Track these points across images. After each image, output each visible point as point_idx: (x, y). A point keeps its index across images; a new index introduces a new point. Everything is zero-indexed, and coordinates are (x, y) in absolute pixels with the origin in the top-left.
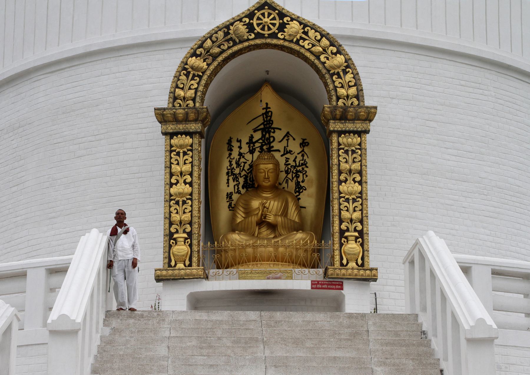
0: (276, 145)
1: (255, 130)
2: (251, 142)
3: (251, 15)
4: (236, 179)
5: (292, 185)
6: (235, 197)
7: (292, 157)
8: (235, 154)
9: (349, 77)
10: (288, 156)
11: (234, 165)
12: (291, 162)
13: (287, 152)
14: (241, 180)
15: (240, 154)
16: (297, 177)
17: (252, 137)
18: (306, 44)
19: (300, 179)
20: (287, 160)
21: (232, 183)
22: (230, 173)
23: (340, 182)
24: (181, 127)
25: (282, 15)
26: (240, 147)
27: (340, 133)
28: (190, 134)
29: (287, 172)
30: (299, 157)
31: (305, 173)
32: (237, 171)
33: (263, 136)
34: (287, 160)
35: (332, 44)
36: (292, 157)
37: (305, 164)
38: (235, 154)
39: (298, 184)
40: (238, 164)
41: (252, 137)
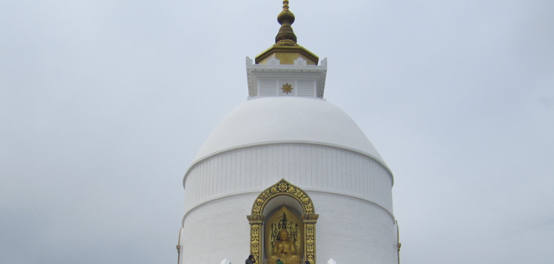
2: (279, 225)
5: (293, 239)
6: (274, 243)
7: (292, 230)
8: (274, 229)
9: (310, 205)
13: (291, 228)
14: (276, 238)
21: (273, 239)
22: (272, 235)
23: (307, 239)
25: (288, 185)
27: (307, 223)
31: (297, 235)
36: (292, 230)
38: (274, 229)
39: (294, 239)
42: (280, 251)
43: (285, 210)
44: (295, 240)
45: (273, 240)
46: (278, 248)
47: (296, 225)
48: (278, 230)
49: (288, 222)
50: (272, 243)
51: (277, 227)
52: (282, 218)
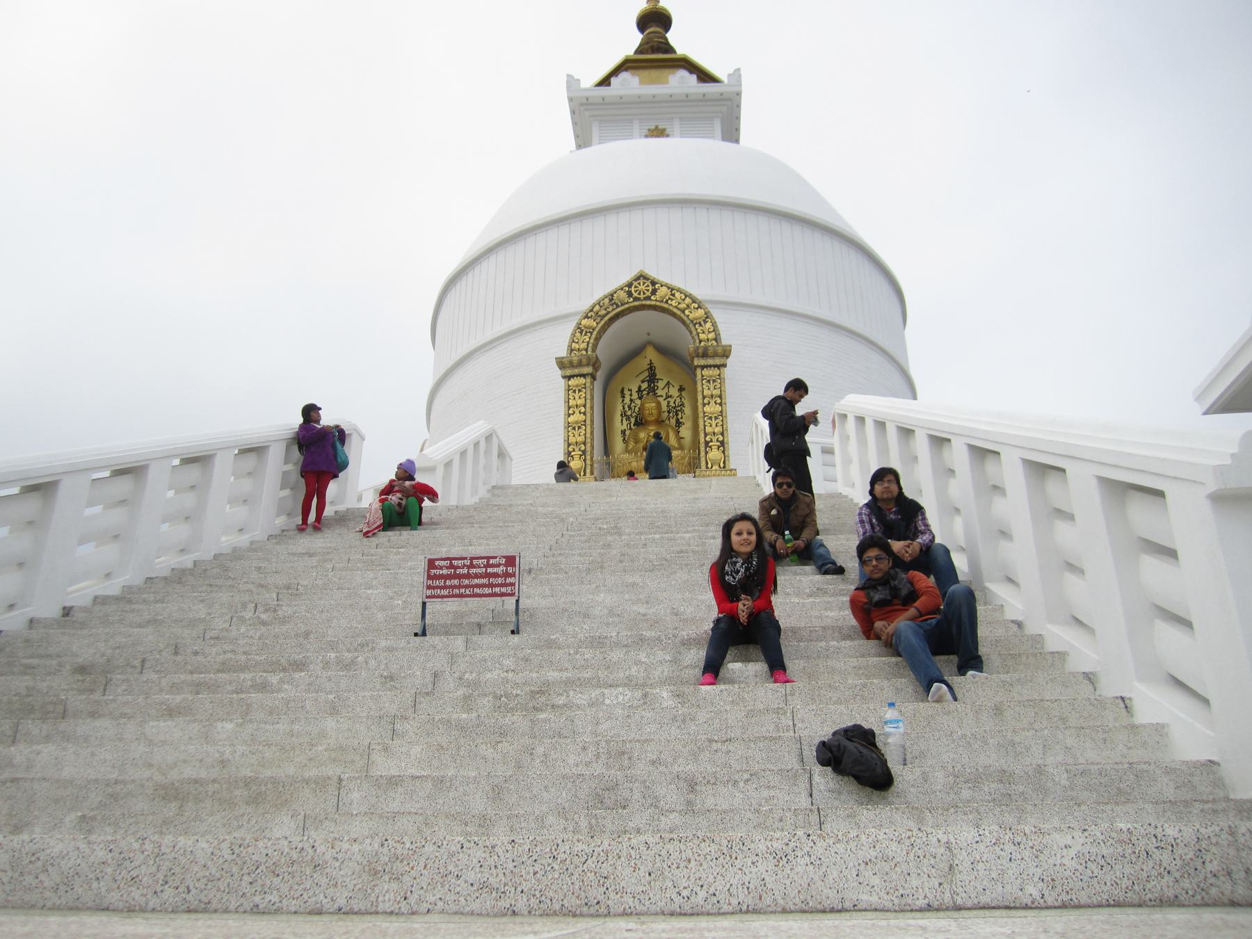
0: (659, 392)
2: (639, 390)
3: (630, 285)
4: (628, 419)
5: (673, 421)
6: (628, 433)
7: (672, 401)
8: (627, 400)
9: (709, 325)
14: (633, 420)
18: (674, 303)
21: (625, 422)
22: (624, 414)
24: (576, 371)
25: (653, 283)
27: (703, 367)
28: (584, 376)
31: (682, 411)
35: (694, 302)
37: (683, 405)
38: (627, 400)
40: (630, 408)
43: (651, 354)
44: (679, 424)
45: (625, 427)
46: (637, 441)
47: (681, 389)
48: (638, 402)
49: (661, 384)
50: (623, 432)
51: (635, 396)
52: (646, 374)
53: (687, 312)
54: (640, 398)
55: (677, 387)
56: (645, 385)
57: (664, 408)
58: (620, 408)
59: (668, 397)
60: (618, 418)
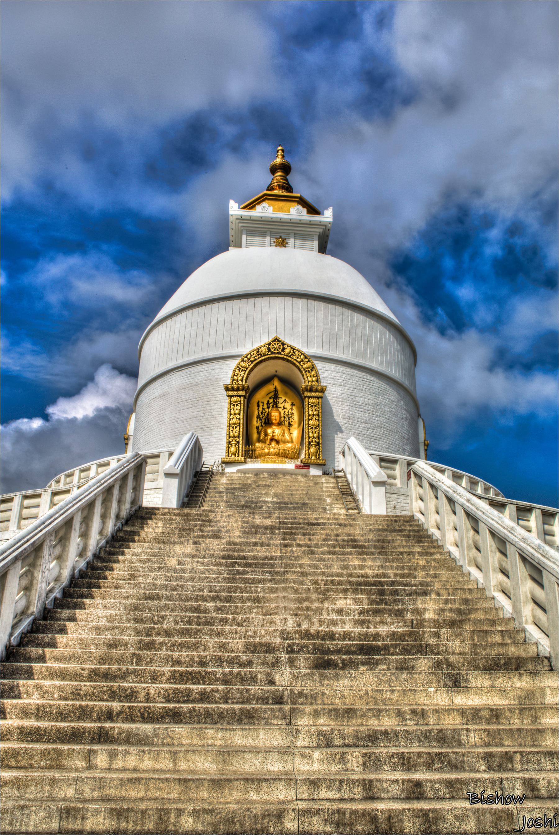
0: (280, 405)
1: (270, 398)
2: (268, 403)
4: (261, 420)
5: (287, 423)
6: (260, 428)
8: (261, 409)
9: (313, 373)
10: (285, 410)
11: (260, 414)
12: (286, 413)
13: (284, 408)
14: (263, 421)
15: (263, 409)
16: (289, 420)
17: (268, 401)
19: (290, 421)
20: (285, 412)
21: (259, 422)
22: (258, 417)
23: (309, 420)
26: (263, 406)
29: (284, 417)
30: (290, 411)
32: (261, 416)
33: (274, 401)
34: (285, 412)
37: (293, 414)
38: (261, 409)
39: (289, 423)
40: (262, 413)
41: (268, 401)
42: (269, 438)
43: (276, 383)
45: (258, 424)
47: (292, 405)
48: (267, 410)
49: (281, 401)
50: (258, 428)
51: (265, 406)
52: (273, 394)
53: (301, 363)
54: (268, 408)
55: (290, 403)
56: (271, 401)
57: (282, 415)
58: (256, 413)
59: (284, 408)
60: (255, 419)
